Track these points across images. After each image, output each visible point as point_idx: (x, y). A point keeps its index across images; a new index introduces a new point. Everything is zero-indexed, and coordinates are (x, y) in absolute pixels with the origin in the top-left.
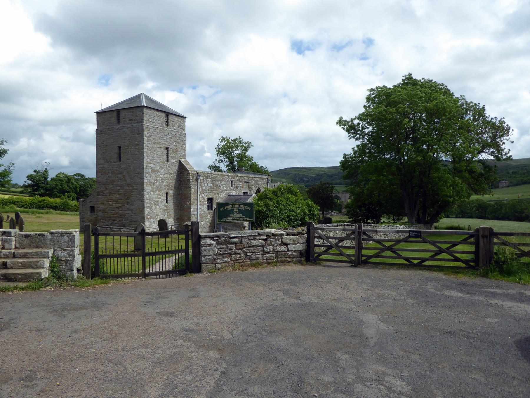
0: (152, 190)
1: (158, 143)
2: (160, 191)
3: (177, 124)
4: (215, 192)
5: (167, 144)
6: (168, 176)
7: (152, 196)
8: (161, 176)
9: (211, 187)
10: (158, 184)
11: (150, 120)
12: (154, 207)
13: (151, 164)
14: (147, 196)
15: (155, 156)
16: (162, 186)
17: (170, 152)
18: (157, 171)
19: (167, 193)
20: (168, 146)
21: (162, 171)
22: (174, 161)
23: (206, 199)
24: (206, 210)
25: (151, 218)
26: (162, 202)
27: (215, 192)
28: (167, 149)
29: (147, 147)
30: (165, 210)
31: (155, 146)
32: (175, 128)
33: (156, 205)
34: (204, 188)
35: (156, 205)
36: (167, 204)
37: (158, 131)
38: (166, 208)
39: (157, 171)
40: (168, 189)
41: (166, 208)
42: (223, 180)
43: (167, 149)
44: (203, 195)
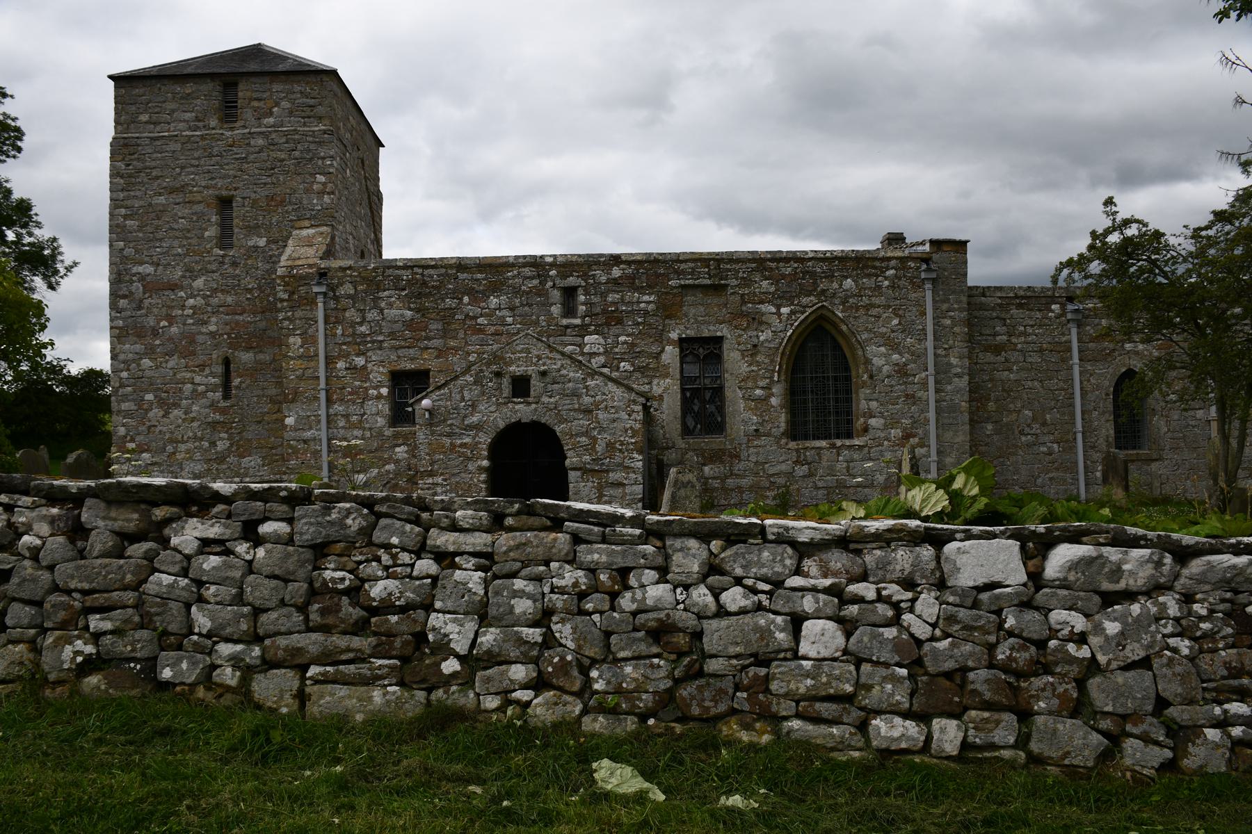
0: (150, 352)
1: (181, 189)
2: (188, 353)
3: (285, 104)
4: (436, 343)
5: (222, 187)
6: (229, 299)
7: (148, 373)
8: (191, 301)
9: (409, 325)
10: (174, 329)
11: (144, 118)
12: (156, 413)
13: (141, 264)
14: (125, 374)
15: (160, 235)
16: (200, 339)
17: (239, 211)
18: (173, 287)
19: (227, 362)
20: (224, 193)
21: (199, 283)
22: (262, 242)
23: (384, 379)
24: (381, 421)
25: (141, 450)
26: (195, 395)
27: (436, 343)
28: (225, 203)
29: (123, 211)
30: (214, 425)
31: (162, 200)
32: (271, 120)
33: (162, 403)
34: (363, 329)
35: (167, 406)
36: (223, 404)
37: (174, 146)
38: (218, 417)
39: (173, 287)
40: (231, 346)
41: (218, 417)
42: (495, 288)
43: (225, 203)
44: (360, 361)
